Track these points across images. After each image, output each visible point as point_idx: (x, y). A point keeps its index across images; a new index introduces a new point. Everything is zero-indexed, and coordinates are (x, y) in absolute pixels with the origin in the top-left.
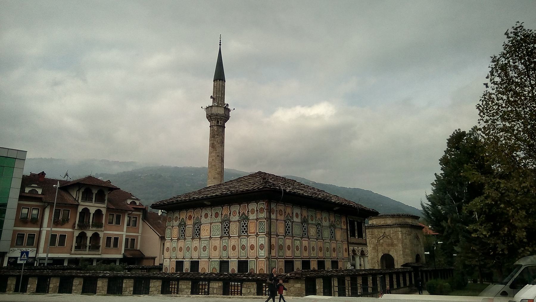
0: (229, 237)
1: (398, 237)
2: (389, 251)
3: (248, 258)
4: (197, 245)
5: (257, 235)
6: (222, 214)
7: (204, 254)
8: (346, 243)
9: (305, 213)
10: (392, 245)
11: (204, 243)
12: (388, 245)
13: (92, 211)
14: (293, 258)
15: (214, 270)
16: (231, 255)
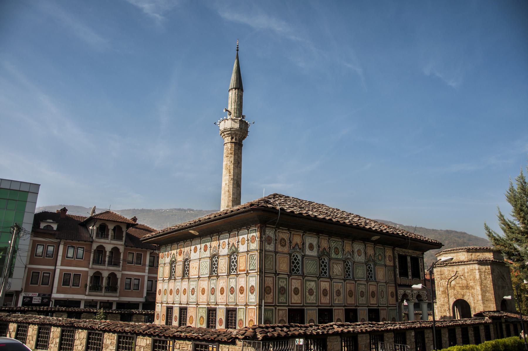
0: (218, 276)
1: (475, 277)
2: (463, 296)
3: (236, 305)
4: (186, 287)
5: (247, 274)
6: (211, 247)
7: (193, 299)
8: (394, 285)
9: (324, 244)
10: (467, 287)
11: (193, 285)
12: (462, 288)
13: (108, 248)
14: (303, 306)
15: (202, 319)
16: (219, 301)
